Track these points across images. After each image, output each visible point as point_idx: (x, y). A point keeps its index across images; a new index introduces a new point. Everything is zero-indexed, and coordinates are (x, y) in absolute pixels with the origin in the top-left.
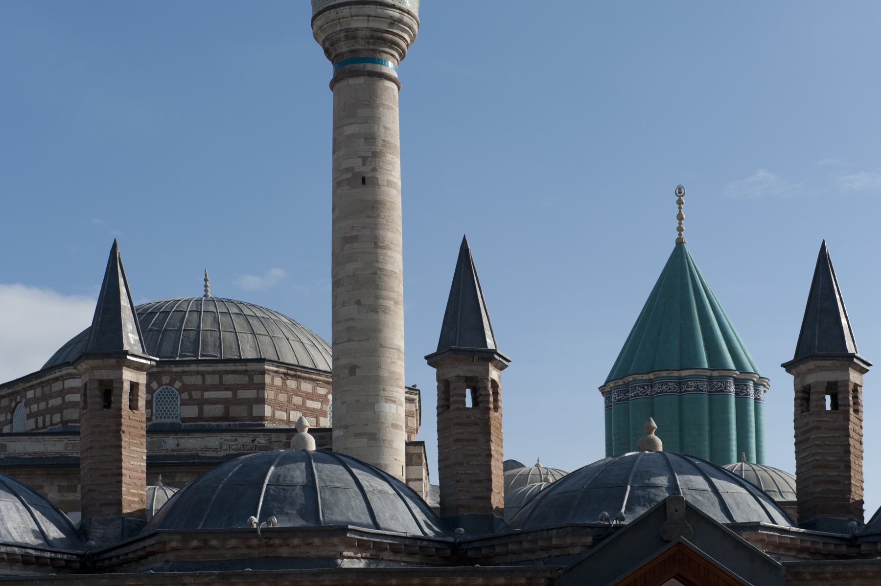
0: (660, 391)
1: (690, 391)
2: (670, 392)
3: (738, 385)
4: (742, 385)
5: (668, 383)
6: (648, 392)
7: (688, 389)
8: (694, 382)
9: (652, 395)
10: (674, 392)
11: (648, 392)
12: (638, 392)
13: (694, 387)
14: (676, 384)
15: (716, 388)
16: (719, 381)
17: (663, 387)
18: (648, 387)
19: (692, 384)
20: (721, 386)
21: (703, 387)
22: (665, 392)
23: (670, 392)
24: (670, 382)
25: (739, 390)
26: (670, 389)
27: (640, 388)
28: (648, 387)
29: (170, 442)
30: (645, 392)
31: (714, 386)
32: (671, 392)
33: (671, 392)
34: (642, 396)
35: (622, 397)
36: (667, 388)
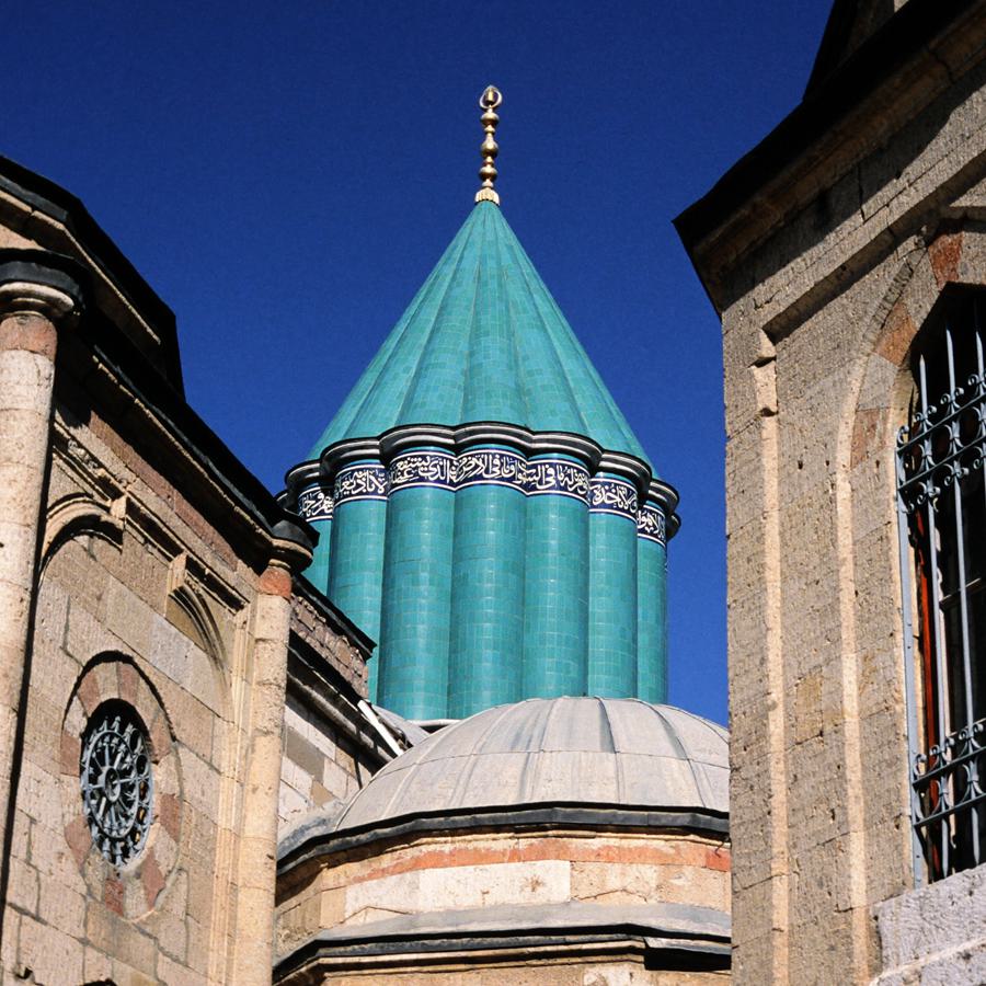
1: (400, 484)
3: (535, 466)
4: (545, 464)
5: (356, 473)
6: (324, 507)
7: (397, 481)
8: (409, 462)
10: (367, 493)
11: (324, 507)
12: (304, 510)
13: (409, 473)
14: (374, 474)
15: (467, 472)
16: (472, 456)
19: (405, 467)
21: (428, 471)
22: (347, 496)
24: (358, 470)
25: (537, 479)
26: (358, 486)
30: (317, 508)
31: (462, 468)
32: (361, 493)
33: (361, 493)
34: (311, 516)
36: (351, 484)
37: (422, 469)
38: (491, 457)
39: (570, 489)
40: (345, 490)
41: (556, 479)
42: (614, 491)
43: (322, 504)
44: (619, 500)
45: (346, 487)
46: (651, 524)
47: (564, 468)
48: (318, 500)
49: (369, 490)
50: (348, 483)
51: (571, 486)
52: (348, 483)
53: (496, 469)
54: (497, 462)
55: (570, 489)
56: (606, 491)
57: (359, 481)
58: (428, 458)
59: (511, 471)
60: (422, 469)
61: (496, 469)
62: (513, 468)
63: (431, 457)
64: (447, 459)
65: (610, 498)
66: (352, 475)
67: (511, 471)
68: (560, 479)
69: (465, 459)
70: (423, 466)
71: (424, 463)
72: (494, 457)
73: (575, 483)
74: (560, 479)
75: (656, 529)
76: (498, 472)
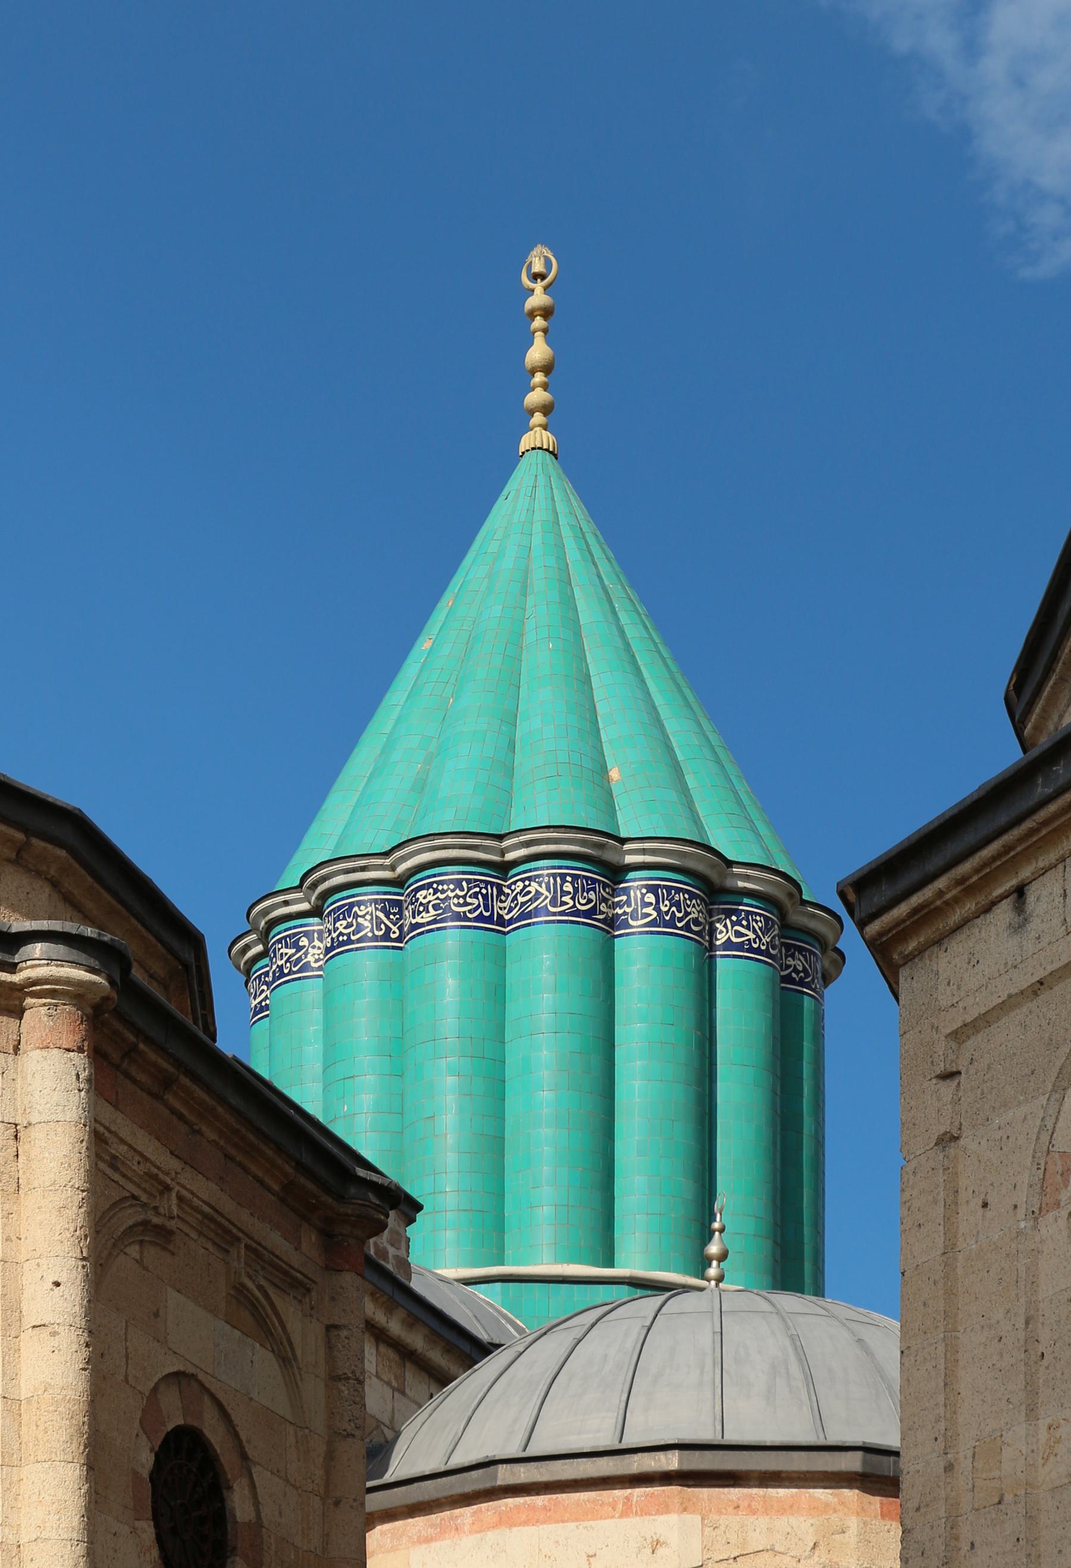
0: (332, 939)
2: (359, 941)
5: (356, 909)
6: (310, 958)
7: (418, 920)
8: (436, 891)
9: (320, 968)
11: (310, 958)
12: (280, 963)
13: (436, 907)
14: (383, 910)
15: (523, 904)
16: (529, 879)
17: (338, 925)
18: (311, 941)
20: (538, 894)
21: (466, 904)
23: (359, 941)
27: (286, 947)
28: (311, 941)
29: (437, 1356)
30: (299, 959)
31: (515, 898)
35: (263, 996)
37: (456, 901)
38: (558, 879)
39: (679, 925)
40: (341, 934)
41: (657, 909)
42: (744, 923)
43: (306, 954)
44: (752, 936)
45: (341, 929)
46: (800, 969)
47: (669, 894)
48: (299, 949)
49: (377, 933)
50: (344, 923)
51: (680, 920)
52: (344, 923)
53: (566, 899)
54: (568, 887)
55: (679, 925)
56: (733, 924)
57: (360, 920)
58: (464, 884)
59: (589, 901)
60: (456, 901)
61: (566, 899)
62: (592, 895)
63: (468, 881)
64: (492, 884)
65: (738, 934)
66: (349, 911)
67: (589, 901)
68: (664, 909)
69: (520, 884)
70: (457, 897)
71: (458, 891)
72: (564, 881)
73: (687, 914)
74: (664, 909)
75: (807, 975)
76: (571, 903)
